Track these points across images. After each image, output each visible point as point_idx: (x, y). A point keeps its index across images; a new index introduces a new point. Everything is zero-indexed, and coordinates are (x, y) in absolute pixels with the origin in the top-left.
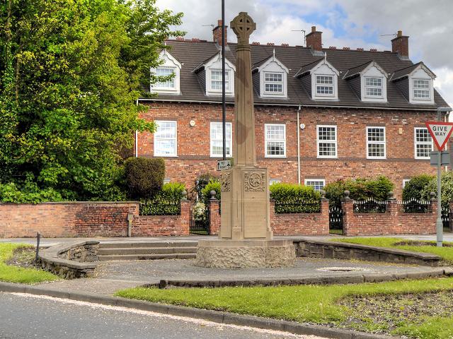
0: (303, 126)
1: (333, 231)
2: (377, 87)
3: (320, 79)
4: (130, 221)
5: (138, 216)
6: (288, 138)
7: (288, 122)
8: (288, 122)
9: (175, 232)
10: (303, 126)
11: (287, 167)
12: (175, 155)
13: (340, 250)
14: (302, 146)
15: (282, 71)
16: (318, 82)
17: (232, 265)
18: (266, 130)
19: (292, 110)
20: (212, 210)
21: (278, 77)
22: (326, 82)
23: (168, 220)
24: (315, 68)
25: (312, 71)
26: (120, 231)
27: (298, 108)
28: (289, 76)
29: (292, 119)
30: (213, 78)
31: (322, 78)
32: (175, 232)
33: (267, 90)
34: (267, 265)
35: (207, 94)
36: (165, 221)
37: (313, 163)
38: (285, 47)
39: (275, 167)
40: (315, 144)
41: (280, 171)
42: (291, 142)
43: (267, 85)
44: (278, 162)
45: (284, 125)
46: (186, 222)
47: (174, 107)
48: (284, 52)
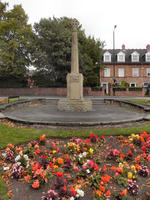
0: (143, 68)
1: (146, 95)
2: (136, 58)
3: (134, 56)
4: (89, 92)
5: (91, 91)
6: (139, 72)
7: (139, 68)
8: (139, 68)
9: (101, 95)
10: (143, 68)
11: (139, 79)
12: (110, 76)
13: (123, 103)
14: (143, 74)
15: (137, 54)
16: (147, 57)
17: (63, 110)
18: (133, 70)
19: (140, 64)
20: (111, 90)
21: (136, 56)
22: (136, 57)
23: (99, 92)
24: (133, 54)
25: (146, 54)
26: (86, 95)
27: (142, 64)
28: (139, 56)
29: (140, 67)
30: (119, 57)
31: (107, 56)
32: (101, 95)
33: (133, 60)
34: (76, 110)
35: (104, 61)
36: (98, 92)
37: (146, 78)
38: (110, 50)
39: (135, 79)
40: (146, 73)
41: (137, 80)
42: (140, 73)
43: (133, 59)
44: (136, 78)
45: (138, 68)
46: (103, 93)
47: (109, 65)
48: (110, 51)
